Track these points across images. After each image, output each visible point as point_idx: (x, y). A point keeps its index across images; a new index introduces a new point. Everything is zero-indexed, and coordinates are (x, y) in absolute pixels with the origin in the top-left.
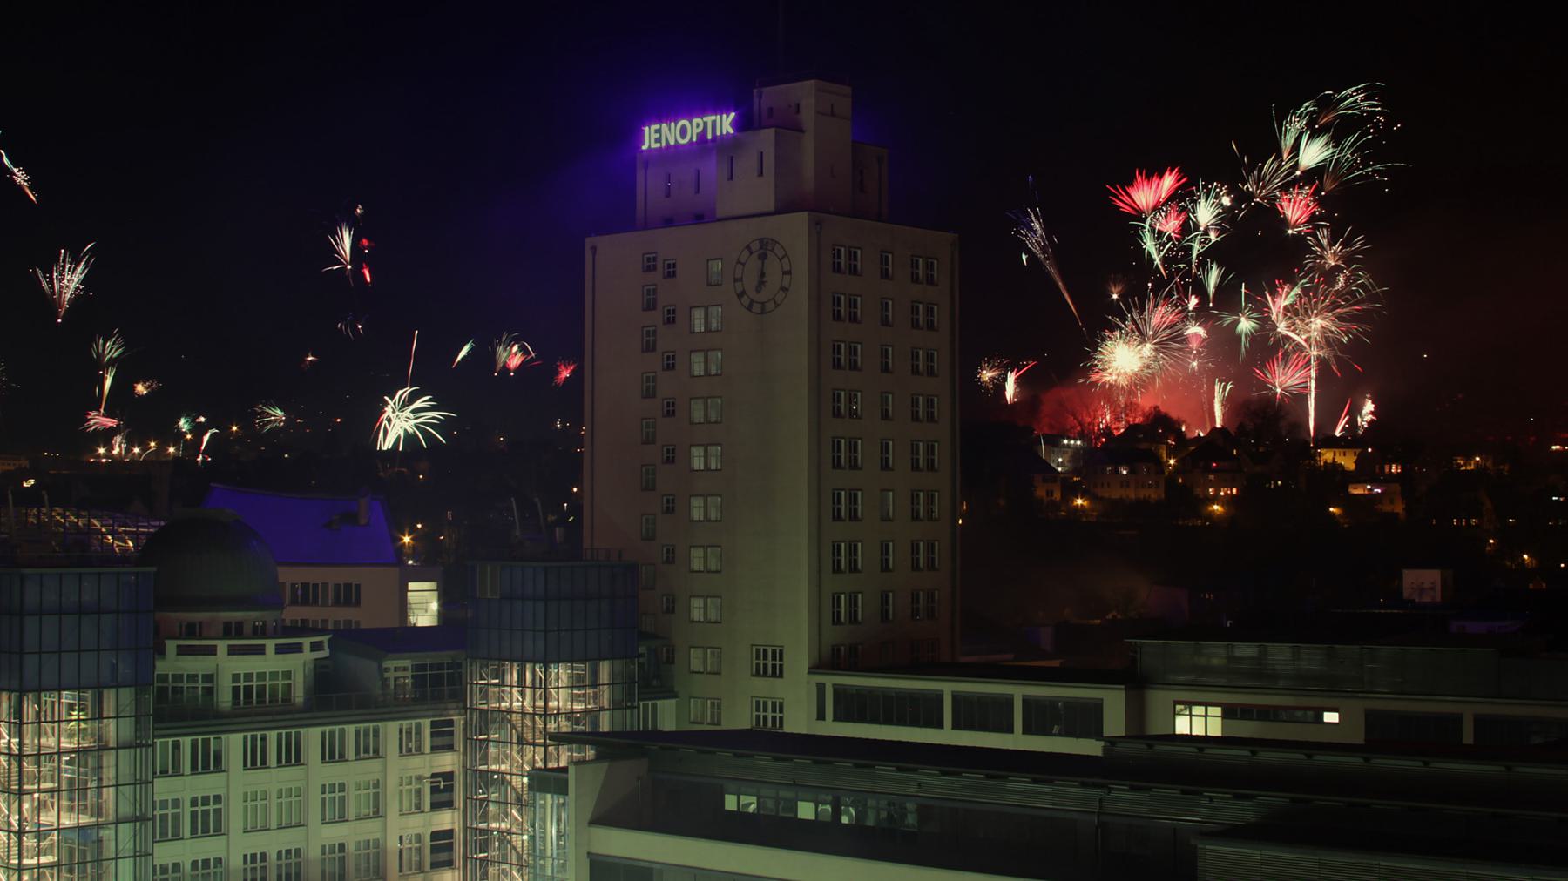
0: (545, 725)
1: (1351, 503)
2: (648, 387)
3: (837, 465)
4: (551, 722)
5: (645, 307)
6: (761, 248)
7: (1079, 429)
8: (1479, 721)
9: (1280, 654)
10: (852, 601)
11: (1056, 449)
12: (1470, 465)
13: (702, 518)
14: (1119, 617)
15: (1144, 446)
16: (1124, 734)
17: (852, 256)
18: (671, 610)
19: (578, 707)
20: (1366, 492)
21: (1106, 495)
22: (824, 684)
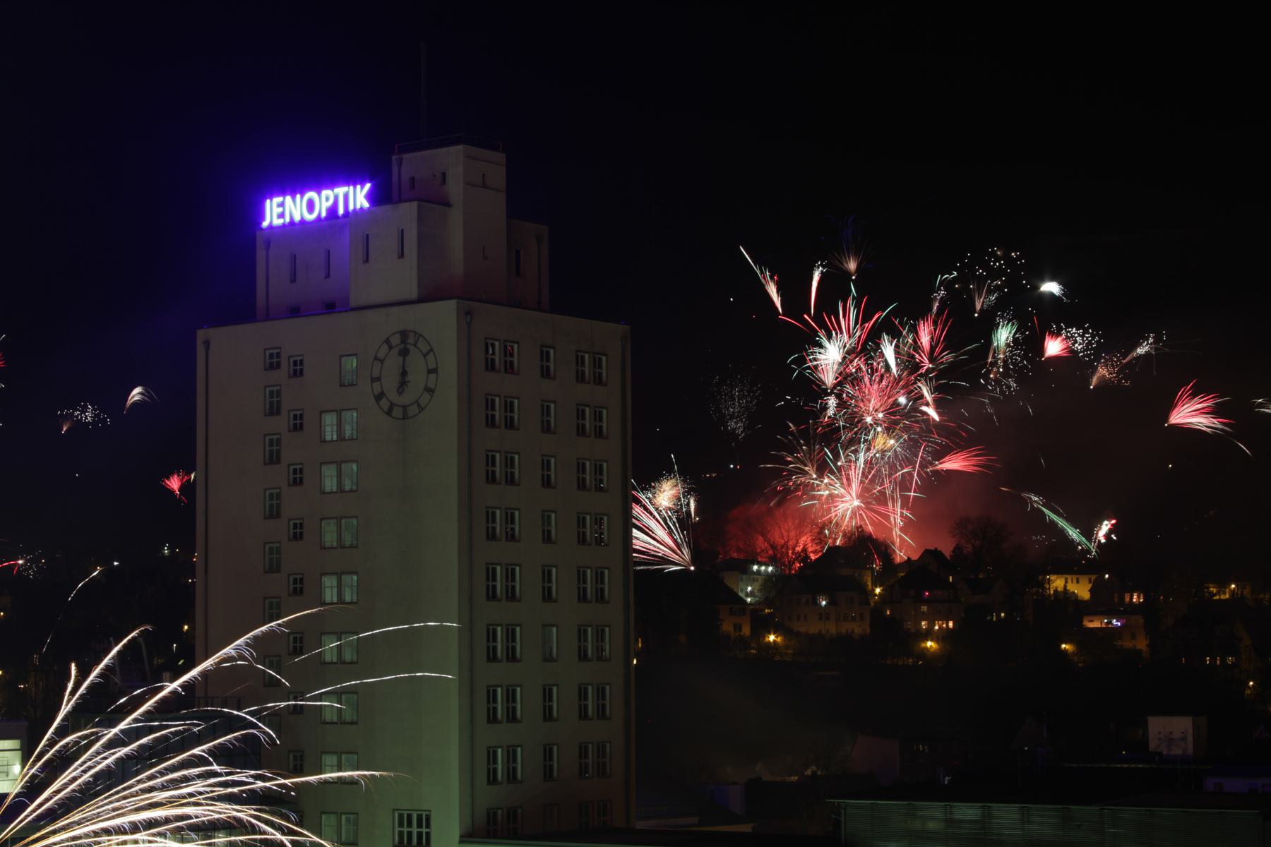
1: (1086, 639)
3: (491, 595)
5: (267, 412)
7: (771, 552)
11: (744, 577)
12: (1225, 593)
14: (819, 773)
17: (508, 353)
20: (1104, 626)
21: (803, 630)
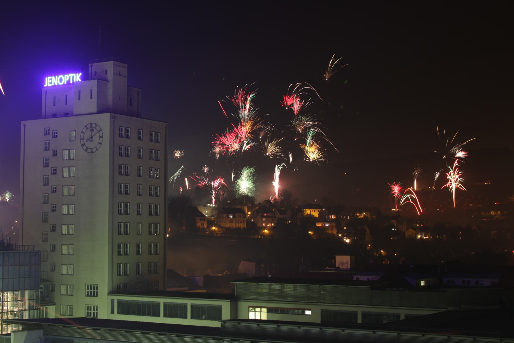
0: (2, 316)
1: (317, 230)
2: (46, 181)
3: (120, 213)
4: (4, 315)
6: (91, 127)
8: (364, 315)
9: (289, 288)
10: (125, 267)
11: (205, 208)
12: (362, 216)
13: (66, 234)
14: (228, 273)
15: (239, 207)
16: (229, 319)
17: (127, 131)
18: (53, 270)
19: (16, 309)
21: (224, 226)
22: (114, 299)
